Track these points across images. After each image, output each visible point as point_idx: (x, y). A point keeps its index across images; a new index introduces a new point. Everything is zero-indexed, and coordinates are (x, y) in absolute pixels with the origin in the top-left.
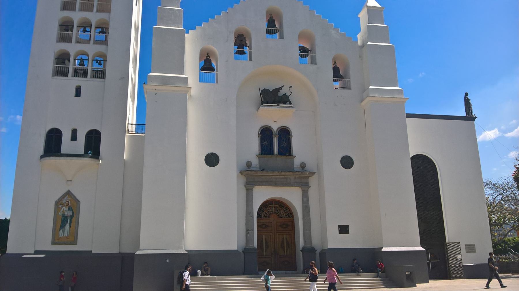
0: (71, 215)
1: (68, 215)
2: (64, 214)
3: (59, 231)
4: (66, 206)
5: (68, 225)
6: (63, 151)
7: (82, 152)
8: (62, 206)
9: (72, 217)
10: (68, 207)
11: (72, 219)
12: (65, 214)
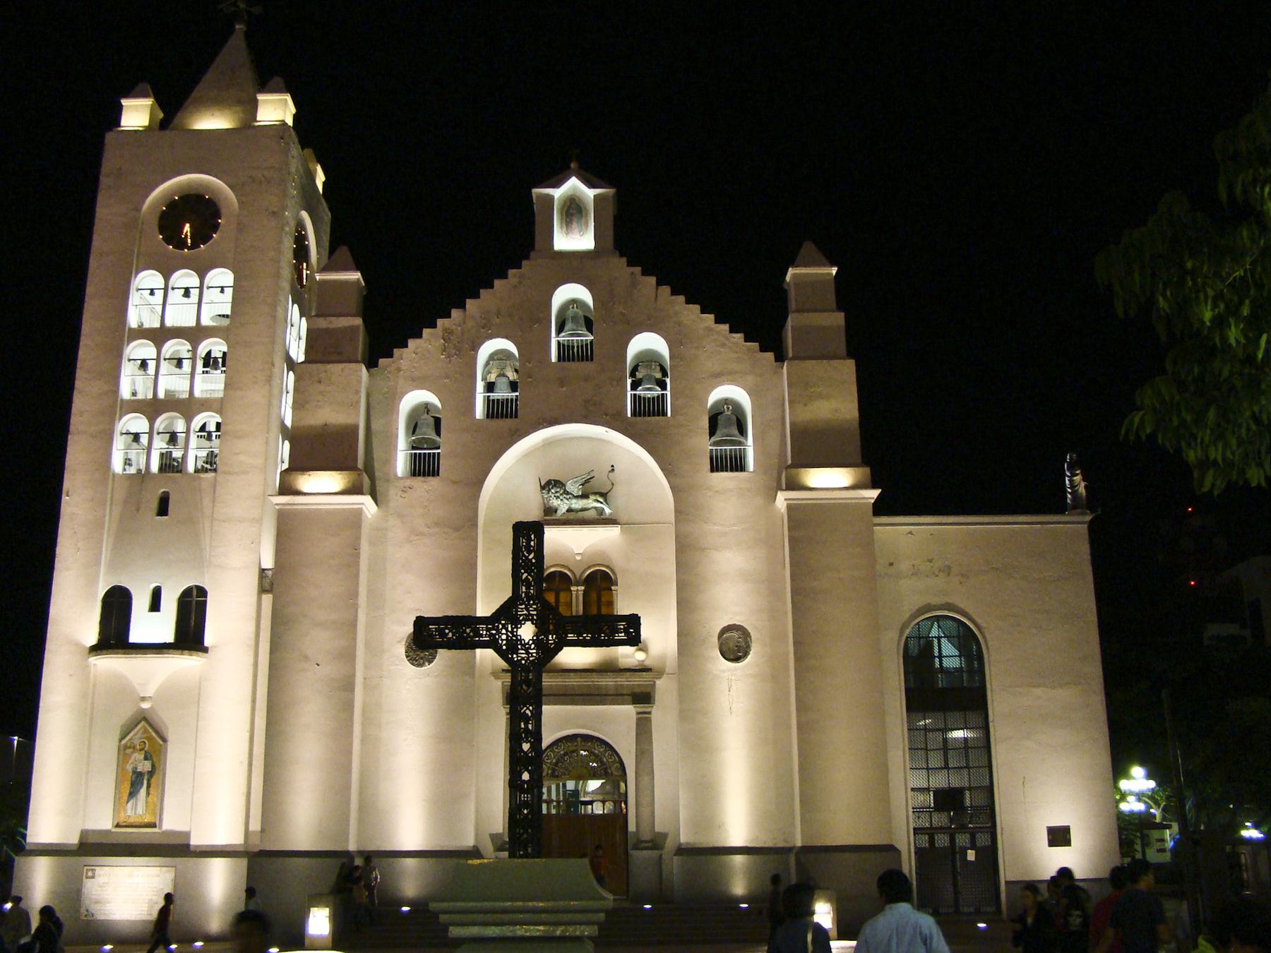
0: (150, 770)
1: (143, 769)
2: (136, 769)
3: (127, 802)
4: (141, 750)
5: (143, 791)
6: (134, 638)
7: (169, 637)
8: (132, 750)
9: (151, 774)
10: (143, 752)
11: (151, 777)
12: (139, 767)
